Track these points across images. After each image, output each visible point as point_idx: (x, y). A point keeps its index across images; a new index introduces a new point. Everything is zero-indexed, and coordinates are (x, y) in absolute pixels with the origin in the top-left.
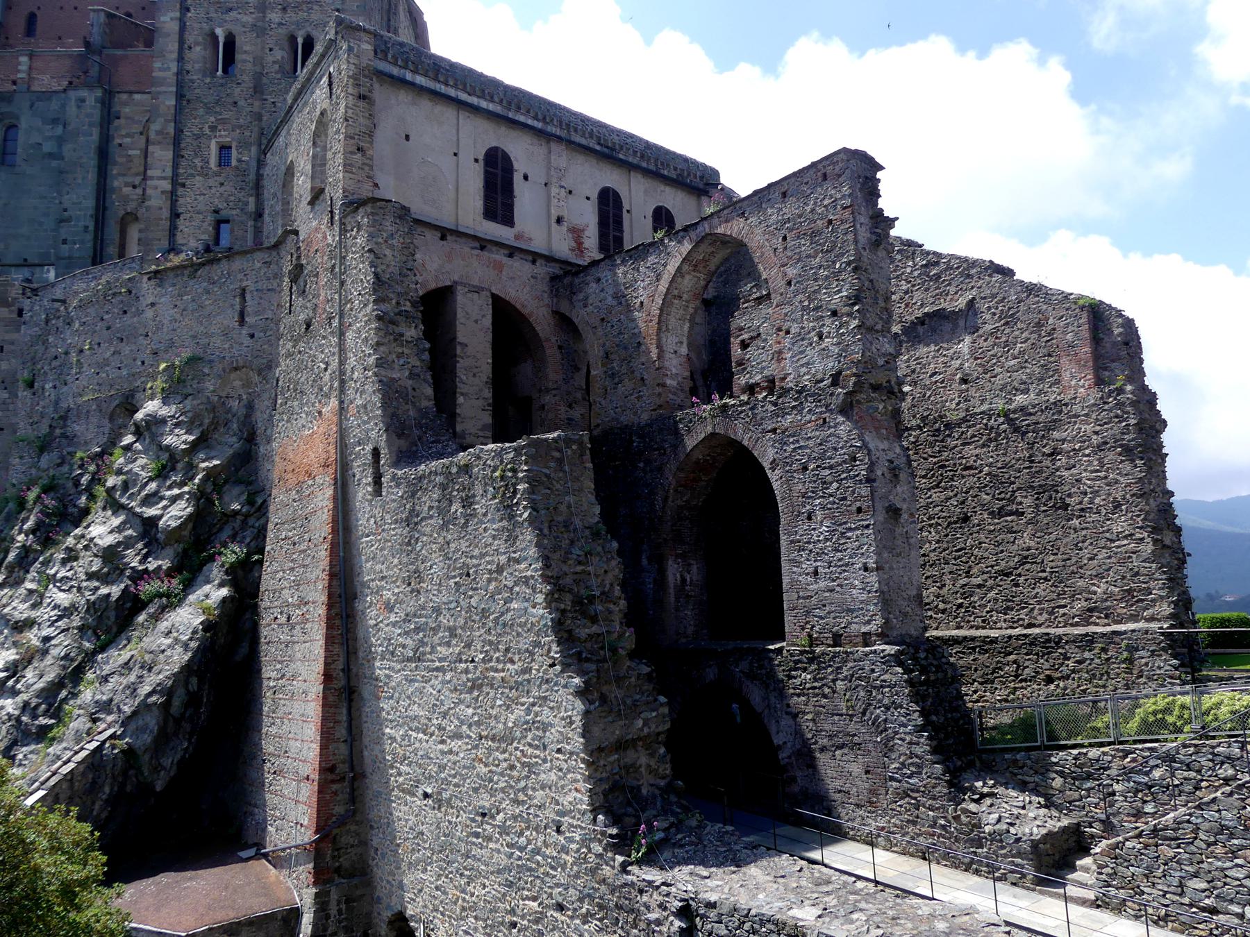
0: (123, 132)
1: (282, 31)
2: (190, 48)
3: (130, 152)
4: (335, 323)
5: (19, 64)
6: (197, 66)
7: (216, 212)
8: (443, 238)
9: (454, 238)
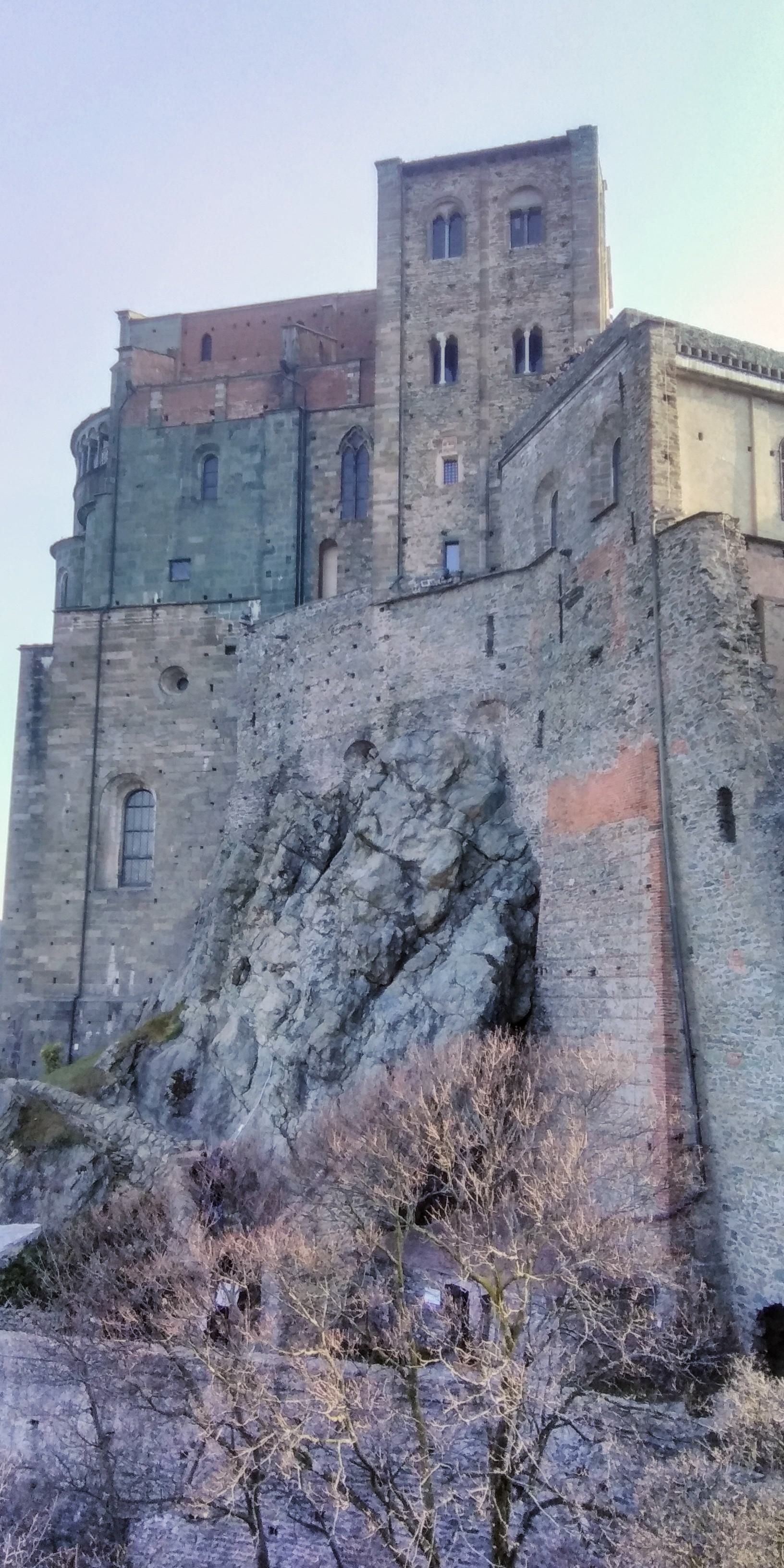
0: (320, 453)
1: (509, 327)
2: (411, 358)
3: (327, 474)
4: (650, 650)
5: (216, 392)
6: (419, 377)
7: (444, 533)
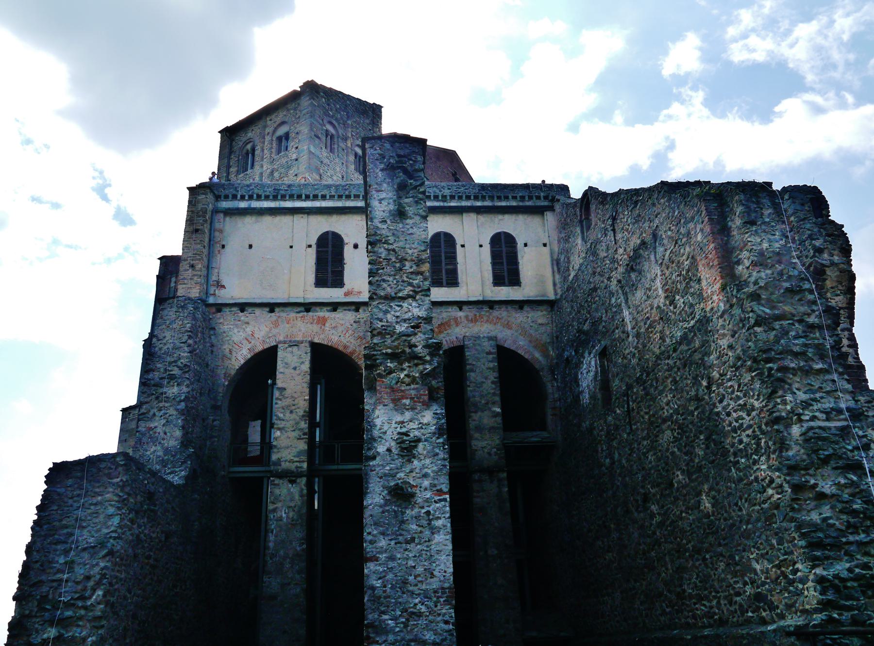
8: (272, 311)
9: (281, 309)
